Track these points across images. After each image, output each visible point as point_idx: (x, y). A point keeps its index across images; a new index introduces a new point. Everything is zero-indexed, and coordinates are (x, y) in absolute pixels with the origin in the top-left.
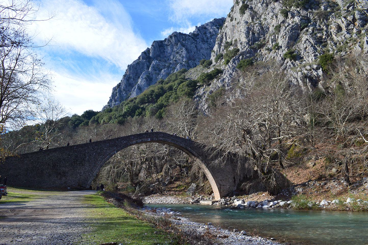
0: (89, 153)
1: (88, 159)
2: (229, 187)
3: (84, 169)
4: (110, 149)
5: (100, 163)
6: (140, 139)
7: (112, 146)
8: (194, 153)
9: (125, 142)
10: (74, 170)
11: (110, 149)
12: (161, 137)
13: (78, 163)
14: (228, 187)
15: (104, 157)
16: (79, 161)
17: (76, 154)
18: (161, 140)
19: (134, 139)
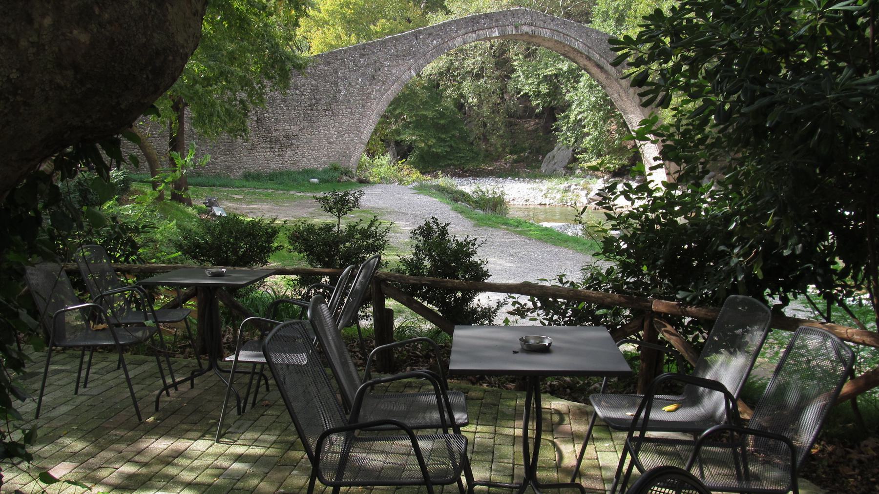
1: (346, 95)
3: (337, 124)
5: (378, 104)
6: (474, 31)
7: (404, 56)
9: (435, 42)
10: (312, 127)
12: (525, 24)
13: (321, 107)
17: (313, 82)
18: (527, 33)
19: (456, 31)
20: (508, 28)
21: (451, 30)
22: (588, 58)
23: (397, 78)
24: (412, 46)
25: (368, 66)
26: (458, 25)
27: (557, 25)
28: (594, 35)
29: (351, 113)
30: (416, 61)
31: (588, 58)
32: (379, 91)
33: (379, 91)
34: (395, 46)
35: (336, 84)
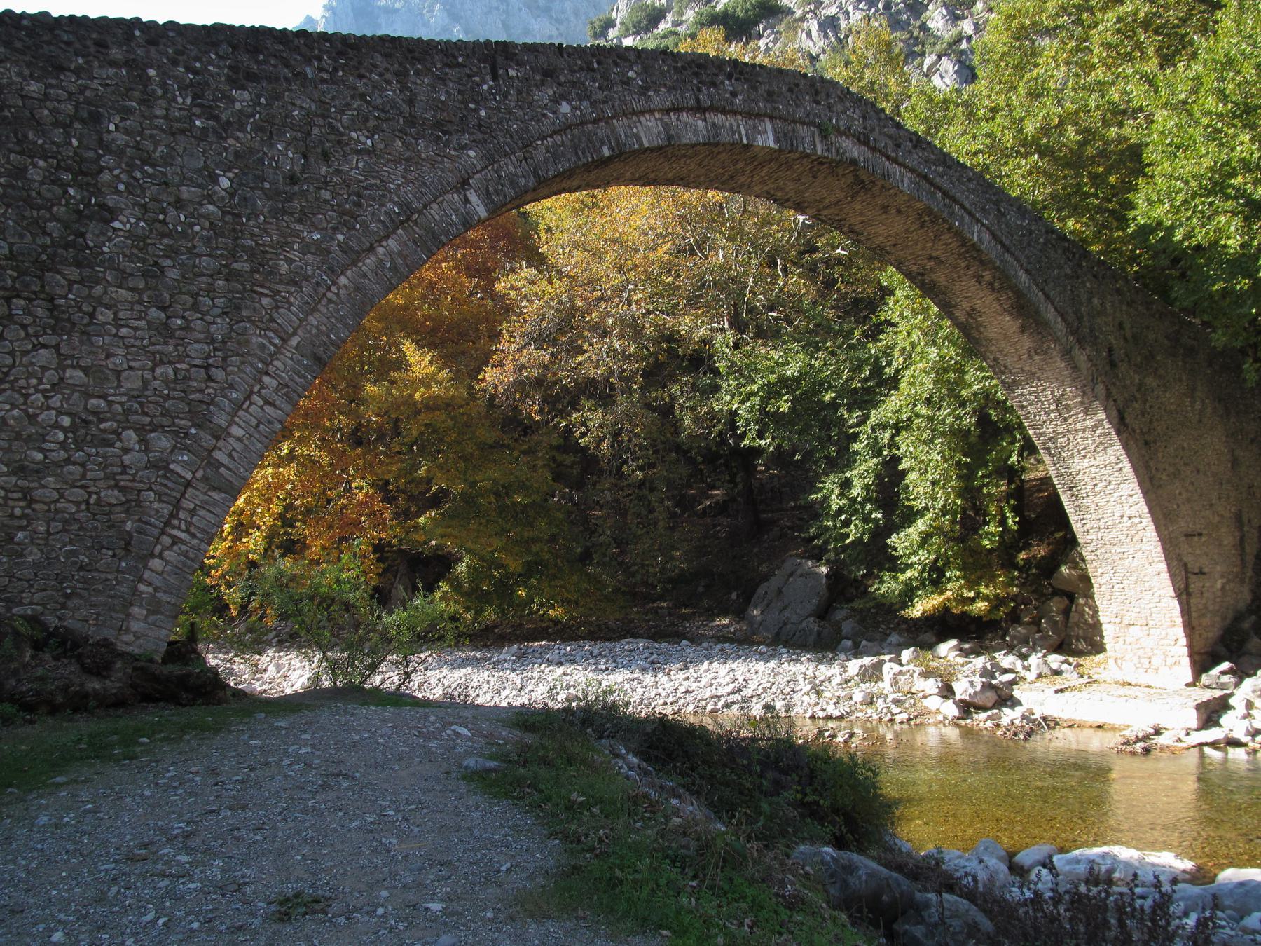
2: (1223, 588)
4: (412, 160)
6: (699, 109)
7: (438, 125)
8: (1049, 313)
9: (565, 108)
11: (412, 160)
14: (1219, 584)
18: (854, 162)
19: (643, 91)
20: (803, 130)
21: (627, 82)
23: (406, 208)
25: (269, 130)
26: (646, 70)
27: (927, 161)
28: (1013, 217)
30: (490, 159)
32: (321, 250)
33: (321, 250)
34: (401, 76)
35: (86, 172)
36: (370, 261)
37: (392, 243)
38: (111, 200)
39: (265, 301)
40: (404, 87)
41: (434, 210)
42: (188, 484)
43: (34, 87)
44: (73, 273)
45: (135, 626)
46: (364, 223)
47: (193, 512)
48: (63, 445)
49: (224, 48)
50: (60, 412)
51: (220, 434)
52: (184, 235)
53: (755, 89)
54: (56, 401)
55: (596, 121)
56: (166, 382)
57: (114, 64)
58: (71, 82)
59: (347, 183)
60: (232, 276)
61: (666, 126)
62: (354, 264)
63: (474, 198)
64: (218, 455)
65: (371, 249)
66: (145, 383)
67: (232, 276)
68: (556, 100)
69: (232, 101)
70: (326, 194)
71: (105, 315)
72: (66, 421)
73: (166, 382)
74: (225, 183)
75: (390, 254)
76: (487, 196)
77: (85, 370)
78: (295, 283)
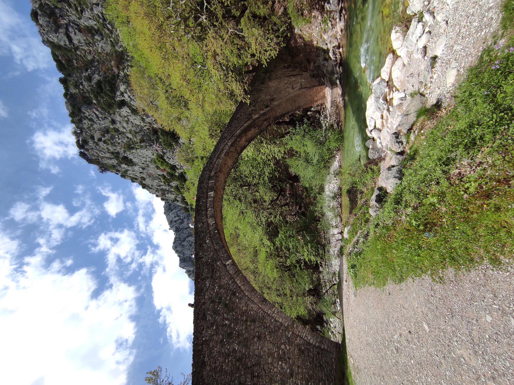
0: (222, 341)
4: (220, 277)
9: (207, 241)
11: (220, 277)
15: (240, 293)
16: (243, 379)
18: (216, 173)
22: (240, 136)
23: (231, 278)
24: (207, 262)
29: (259, 338)
30: (219, 260)
31: (240, 136)
33: (240, 299)
36: (242, 287)
37: (238, 282)
38: (231, 350)
39: (252, 313)
40: (205, 279)
41: (231, 272)
42: (293, 333)
43: (208, 368)
44: (247, 360)
45: (326, 348)
46: (234, 289)
47: (299, 332)
48: (286, 364)
49: (198, 322)
50: (278, 364)
51: (281, 324)
52: (238, 332)
53: (202, 197)
54: (276, 365)
55: (210, 234)
56: (270, 337)
57: (202, 348)
58: (206, 359)
59: (226, 293)
60: (246, 321)
61: (210, 217)
62: (243, 291)
63: (227, 263)
64: (286, 325)
65: (240, 287)
66: (271, 342)
67: (246, 321)
68: (206, 243)
69: (209, 320)
70: (228, 298)
71: (256, 352)
72: (280, 363)
73: (270, 337)
74: (227, 322)
75: (240, 282)
76: (227, 260)
77: (269, 358)
78: (248, 305)
